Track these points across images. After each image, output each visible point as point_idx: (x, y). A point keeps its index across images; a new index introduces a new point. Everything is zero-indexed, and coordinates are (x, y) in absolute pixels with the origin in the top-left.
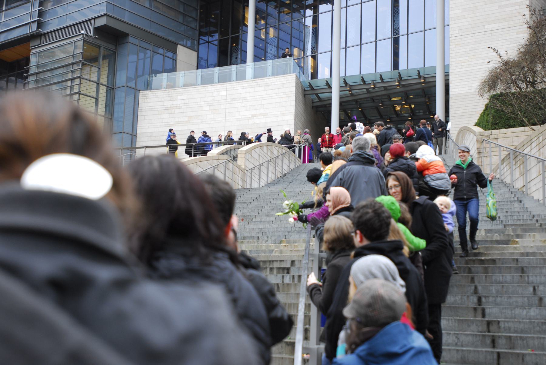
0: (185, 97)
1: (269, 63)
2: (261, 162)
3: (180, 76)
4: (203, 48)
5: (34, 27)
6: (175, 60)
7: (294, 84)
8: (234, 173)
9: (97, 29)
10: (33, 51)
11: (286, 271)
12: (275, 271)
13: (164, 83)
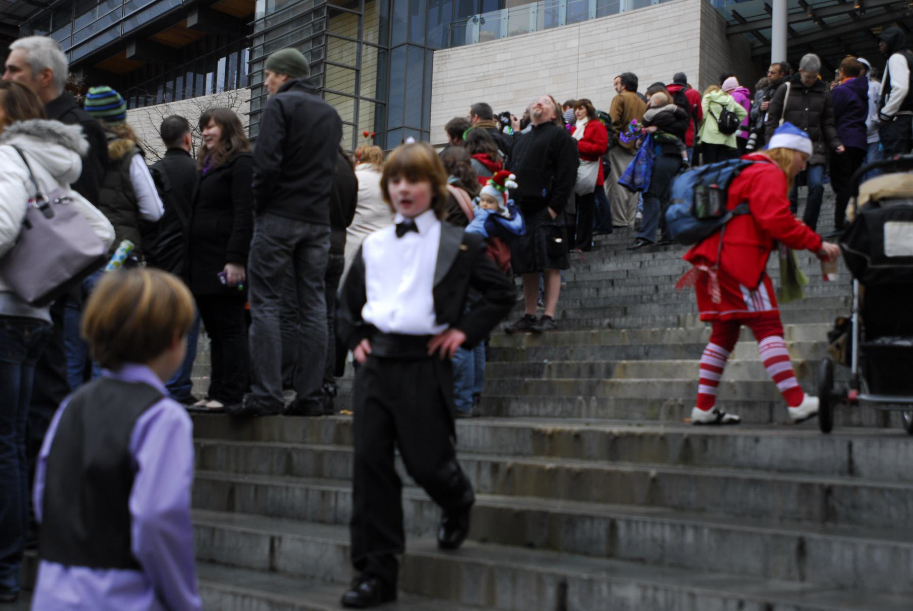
0: (508, 56)
7: (698, 15)
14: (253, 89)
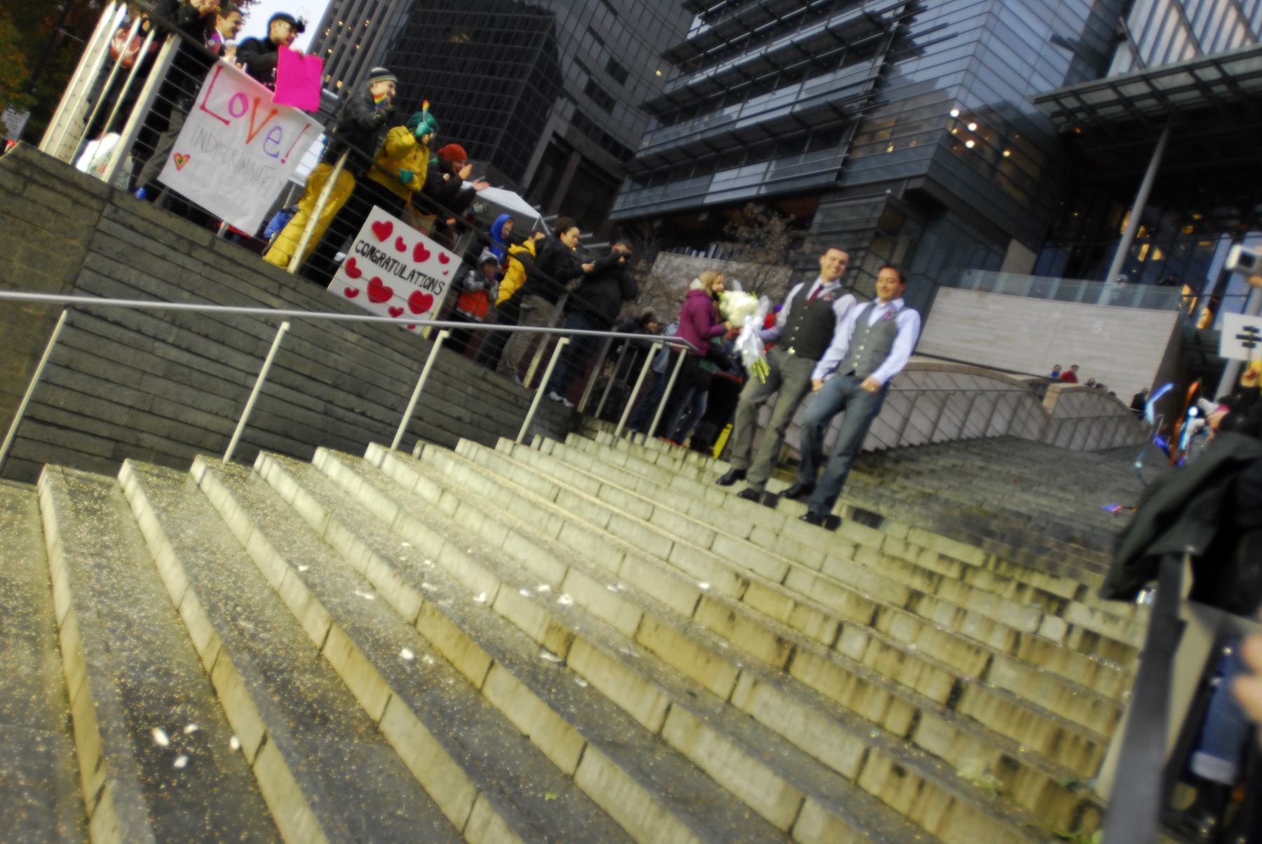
1: (1142, 289)
2: (1083, 414)
3: (1003, 278)
4: (1048, 253)
5: (833, 178)
6: (1002, 258)
8: (1030, 414)
9: (910, 194)
10: (822, 206)
11: (1054, 607)
12: (1028, 596)
13: (977, 284)
14: (795, 271)
